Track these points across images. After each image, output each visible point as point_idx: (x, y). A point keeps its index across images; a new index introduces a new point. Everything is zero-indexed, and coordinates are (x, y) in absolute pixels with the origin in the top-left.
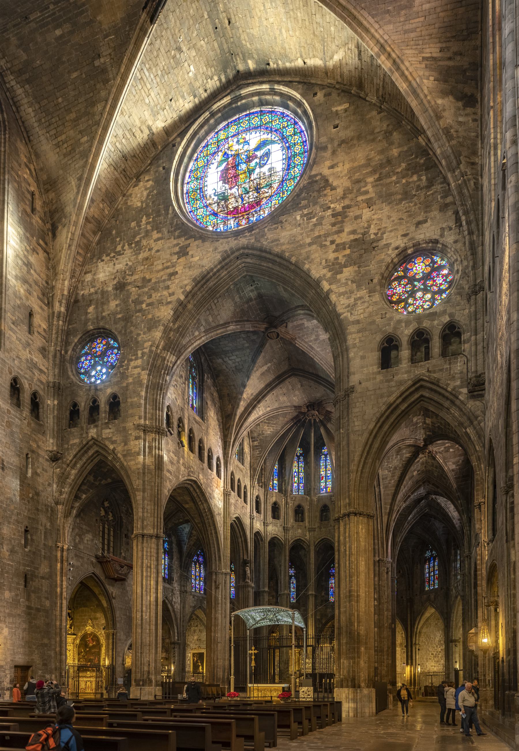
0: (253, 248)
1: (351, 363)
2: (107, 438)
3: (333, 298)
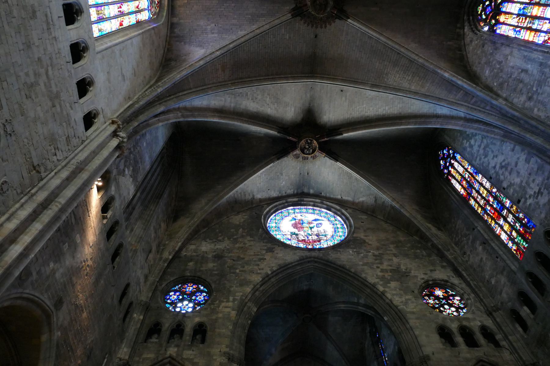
0: (321, 259)
1: (419, 339)
2: (187, 359)
3: (389, 296)
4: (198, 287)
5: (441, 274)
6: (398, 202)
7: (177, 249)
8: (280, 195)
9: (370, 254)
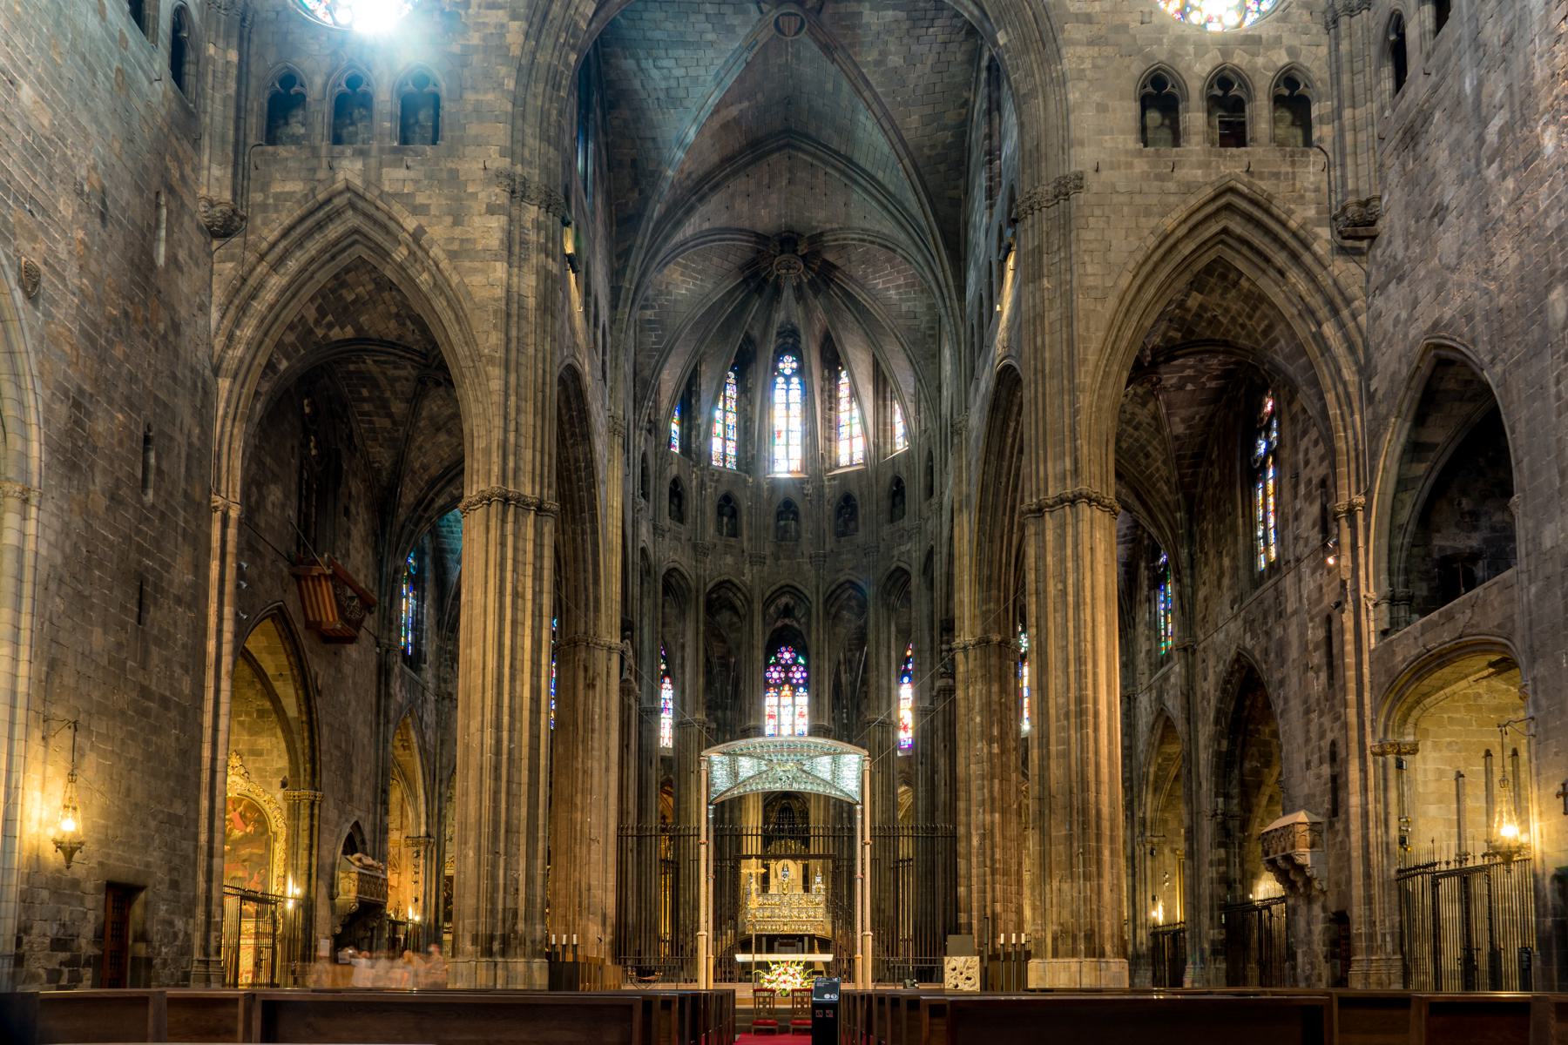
2: (397, 196)
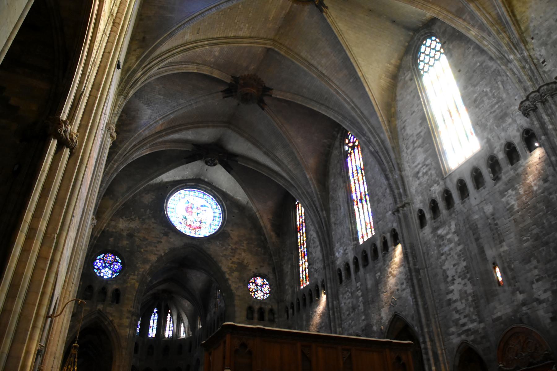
3: (230, 282)
4: (115, 258)
5: (264, 271)
6: (259, 214)
7: (103, 229)
8: (182, 179)
9: (230, 247)
